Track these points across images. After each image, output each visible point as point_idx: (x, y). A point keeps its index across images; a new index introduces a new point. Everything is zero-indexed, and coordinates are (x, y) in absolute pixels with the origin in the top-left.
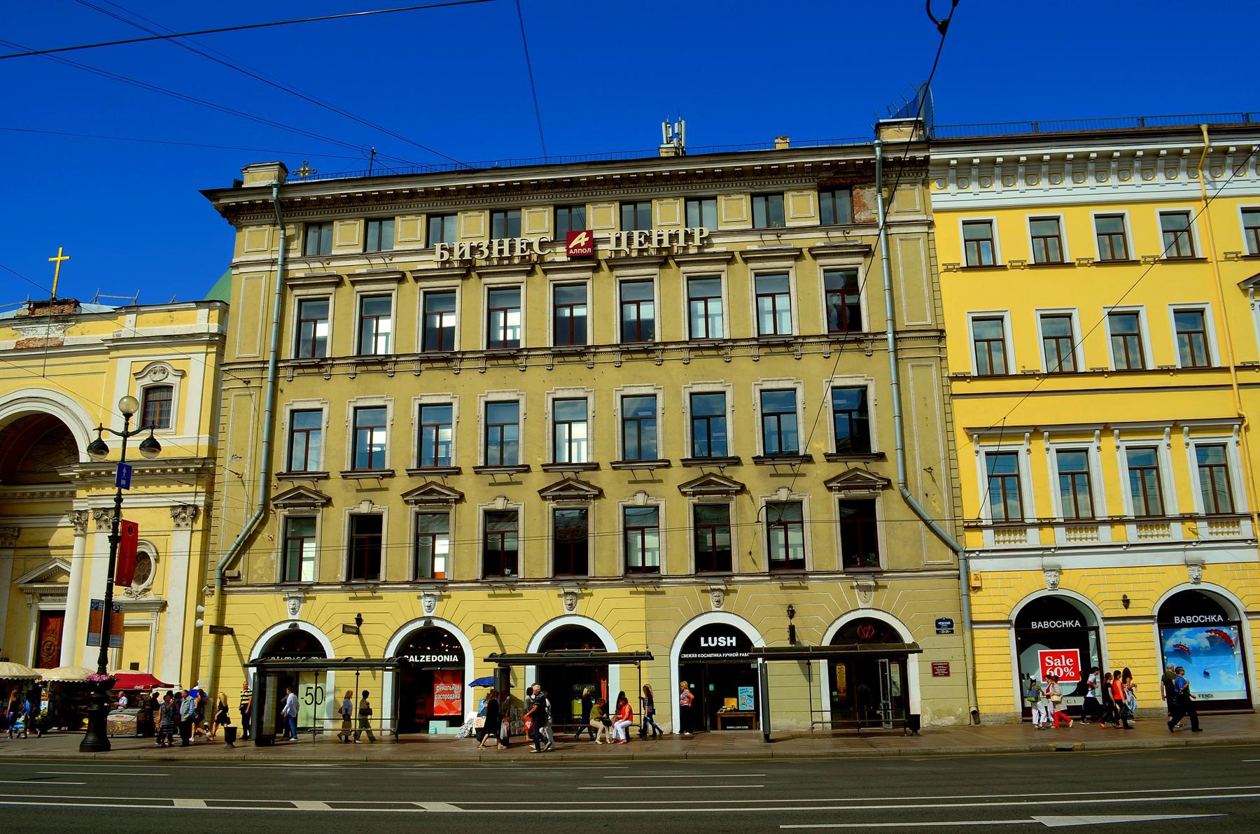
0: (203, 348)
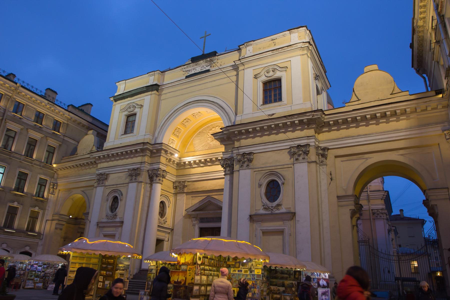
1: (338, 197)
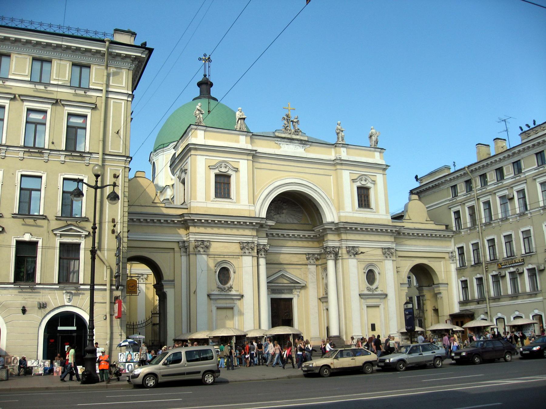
0: (381, 171)
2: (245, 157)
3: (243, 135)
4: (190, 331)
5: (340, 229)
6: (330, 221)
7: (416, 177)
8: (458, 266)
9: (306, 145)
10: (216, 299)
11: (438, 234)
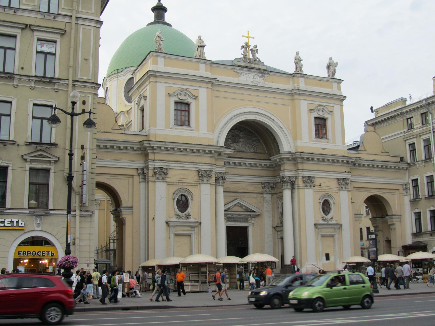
0: (338, 102)
1: (355, 214)
2: (204, 85)
3: (204, 63)
4: (147, 258)
5: (297, 159)
6: (287, 151)
7: (372, 108)
8: (412, 198)
9: (265, 74)
10: (174, 227)
11: (393, 165)
